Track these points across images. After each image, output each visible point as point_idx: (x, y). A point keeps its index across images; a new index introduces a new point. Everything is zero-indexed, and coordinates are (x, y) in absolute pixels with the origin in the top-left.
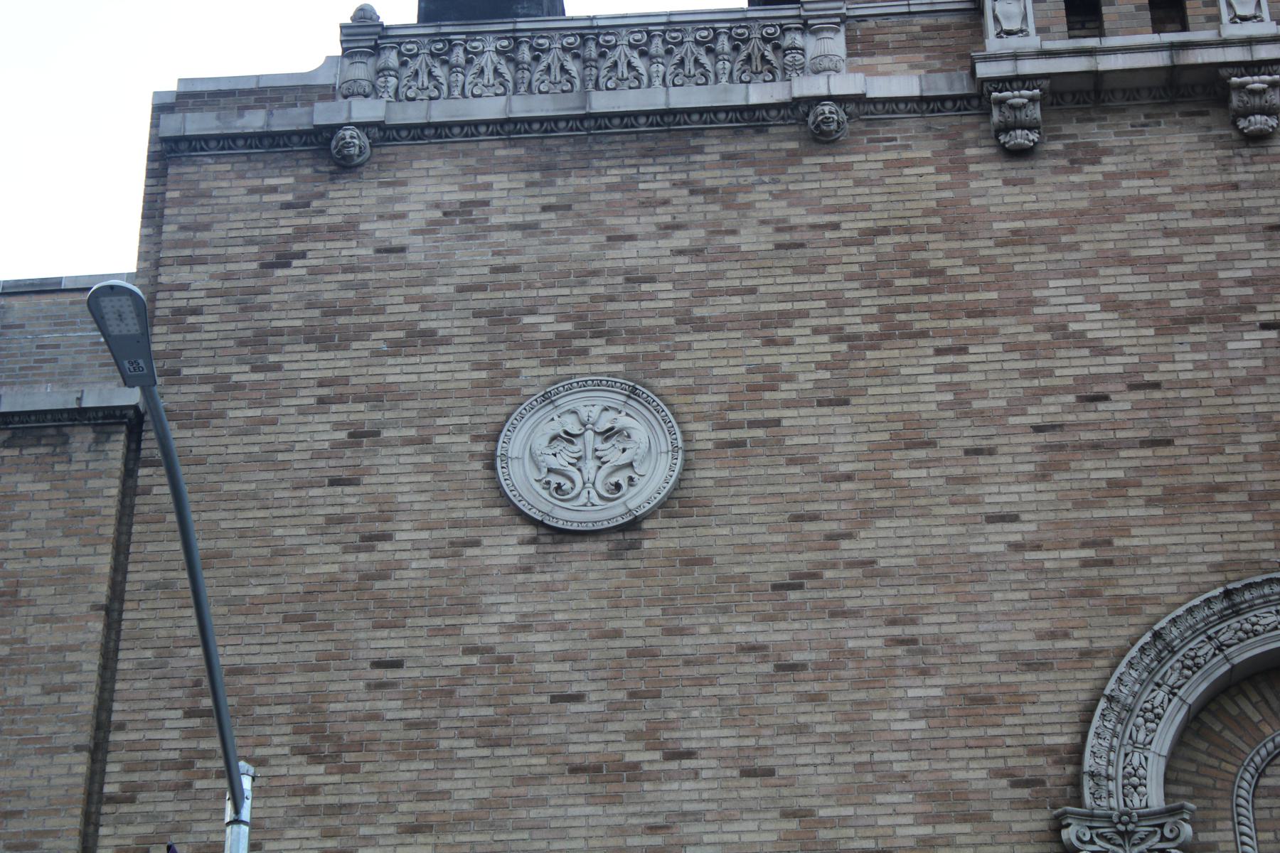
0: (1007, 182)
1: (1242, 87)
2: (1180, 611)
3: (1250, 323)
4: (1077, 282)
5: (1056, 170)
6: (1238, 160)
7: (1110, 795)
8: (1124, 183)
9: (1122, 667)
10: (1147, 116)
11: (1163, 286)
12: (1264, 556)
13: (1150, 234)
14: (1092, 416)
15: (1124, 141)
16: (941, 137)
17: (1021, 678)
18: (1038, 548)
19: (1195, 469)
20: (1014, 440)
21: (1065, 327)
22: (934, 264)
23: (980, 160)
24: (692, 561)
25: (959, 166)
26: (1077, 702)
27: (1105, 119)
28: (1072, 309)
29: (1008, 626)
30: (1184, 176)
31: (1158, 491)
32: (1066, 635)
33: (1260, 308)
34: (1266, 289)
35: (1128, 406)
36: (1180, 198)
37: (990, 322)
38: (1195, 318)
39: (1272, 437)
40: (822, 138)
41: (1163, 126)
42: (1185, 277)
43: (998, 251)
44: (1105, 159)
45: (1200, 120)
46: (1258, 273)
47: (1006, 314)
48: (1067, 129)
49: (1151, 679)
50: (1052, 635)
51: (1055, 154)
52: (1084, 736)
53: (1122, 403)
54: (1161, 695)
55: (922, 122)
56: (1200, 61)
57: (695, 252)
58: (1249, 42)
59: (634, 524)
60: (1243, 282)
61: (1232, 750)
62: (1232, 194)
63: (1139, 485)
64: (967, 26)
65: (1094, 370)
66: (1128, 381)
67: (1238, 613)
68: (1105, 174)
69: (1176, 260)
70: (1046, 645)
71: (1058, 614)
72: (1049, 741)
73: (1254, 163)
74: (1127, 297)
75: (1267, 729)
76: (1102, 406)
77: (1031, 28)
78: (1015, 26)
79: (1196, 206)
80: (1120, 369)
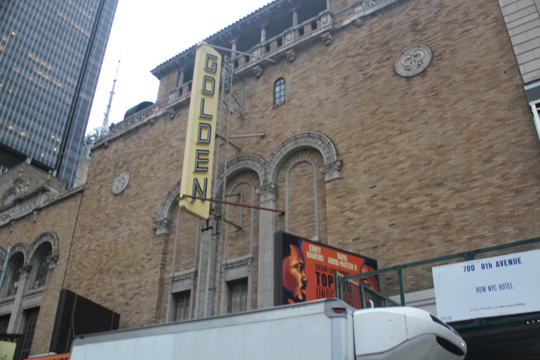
24: (128, 195)
40: (152, 124)
57: (137, 148)
59: (123, 191)
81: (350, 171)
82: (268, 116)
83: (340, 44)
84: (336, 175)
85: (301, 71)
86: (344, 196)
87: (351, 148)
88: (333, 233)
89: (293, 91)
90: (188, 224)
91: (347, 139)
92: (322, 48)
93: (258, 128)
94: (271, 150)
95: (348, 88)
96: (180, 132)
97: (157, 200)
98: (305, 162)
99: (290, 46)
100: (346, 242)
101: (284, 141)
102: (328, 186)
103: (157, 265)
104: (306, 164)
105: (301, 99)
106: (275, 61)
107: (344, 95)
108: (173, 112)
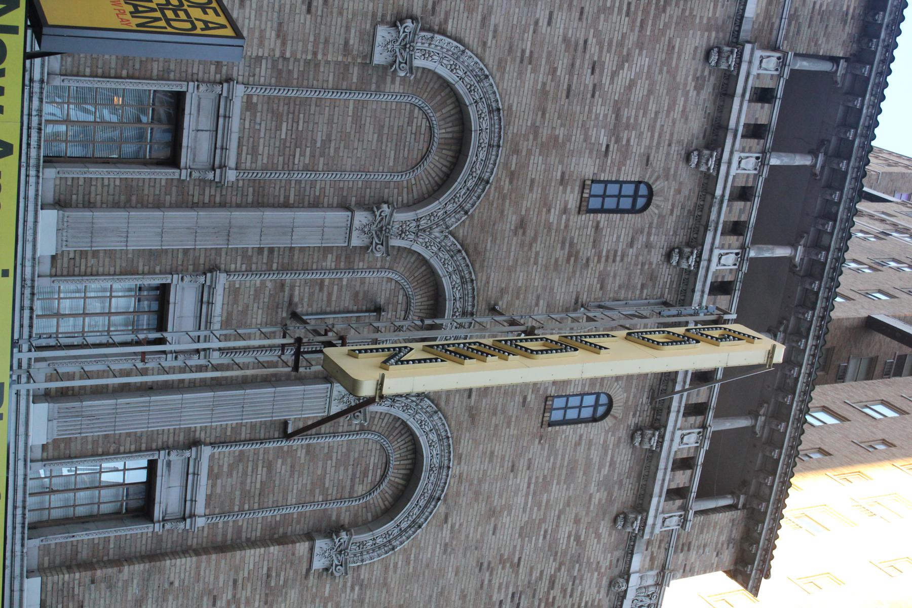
0: (696, 48)
1: (711, 156)
2: (495, 88)
4: (645, 71)
5: (696, 70)
7: (423, 43)
8: (683, 99)
9: (476, 59)
12: (511, 128)
14: (586, 66)
15: (701, 102)
16: (723, 22)
17: (480, 14)
18: (534, 32)
19: (554, 106)
20: (583, 30)
21: (627, 61)
22: (668, 9)
23: (709, 38)
25: (708, 28)
26: (465, 37)
29: (503, 12)
30: (679, 125)
31: (548, 88)
32: (494, 37)
35: (587, 82)
37: (637, 29)
38: (618, 118)
39: (560, 141)
42: (636, 117)
43: (667, 39)
44: (695, 92)
45: (701, 136)
47: (639, 36)
48: (712, 79)
49: (468, 70)
50: (495, 31)
51: (703, 71)
52: (450, 37)
53: (589, 80)
54: (461, 73)
55: (732, 16)
58: (729, 163)
60: (628, 141)
61: (432, 98)
62: (667, 142)
63: (552, 81)
64: (769, 43)
67: (489, 112)
68: (688, 92)
69: (645, 114)
70: (492, 28)
71: (504, 35)
72: (450, 21)
75: (438, 114)
76: (589, 71)
77: (761, 72)
78: (763, 65)
80: (604, 81)
81: (314, 590)
83: (601, 549)
84: (319, 564)
85: (596, 459)
86: (267, 583)
87: (361, 589)
88: (198, 567)
89: (559, 444)
90: (370, 134)
91: (385, 579)
94: (447, 402)
97: (484, 20)
98: (384, 476)
99: (666, 445)
100: (170, 598)
101: (451, 442)
102: (302, 548)
103: (284, 44)
104: (378, 479)
105: (528, 468)
107: (482, 564)
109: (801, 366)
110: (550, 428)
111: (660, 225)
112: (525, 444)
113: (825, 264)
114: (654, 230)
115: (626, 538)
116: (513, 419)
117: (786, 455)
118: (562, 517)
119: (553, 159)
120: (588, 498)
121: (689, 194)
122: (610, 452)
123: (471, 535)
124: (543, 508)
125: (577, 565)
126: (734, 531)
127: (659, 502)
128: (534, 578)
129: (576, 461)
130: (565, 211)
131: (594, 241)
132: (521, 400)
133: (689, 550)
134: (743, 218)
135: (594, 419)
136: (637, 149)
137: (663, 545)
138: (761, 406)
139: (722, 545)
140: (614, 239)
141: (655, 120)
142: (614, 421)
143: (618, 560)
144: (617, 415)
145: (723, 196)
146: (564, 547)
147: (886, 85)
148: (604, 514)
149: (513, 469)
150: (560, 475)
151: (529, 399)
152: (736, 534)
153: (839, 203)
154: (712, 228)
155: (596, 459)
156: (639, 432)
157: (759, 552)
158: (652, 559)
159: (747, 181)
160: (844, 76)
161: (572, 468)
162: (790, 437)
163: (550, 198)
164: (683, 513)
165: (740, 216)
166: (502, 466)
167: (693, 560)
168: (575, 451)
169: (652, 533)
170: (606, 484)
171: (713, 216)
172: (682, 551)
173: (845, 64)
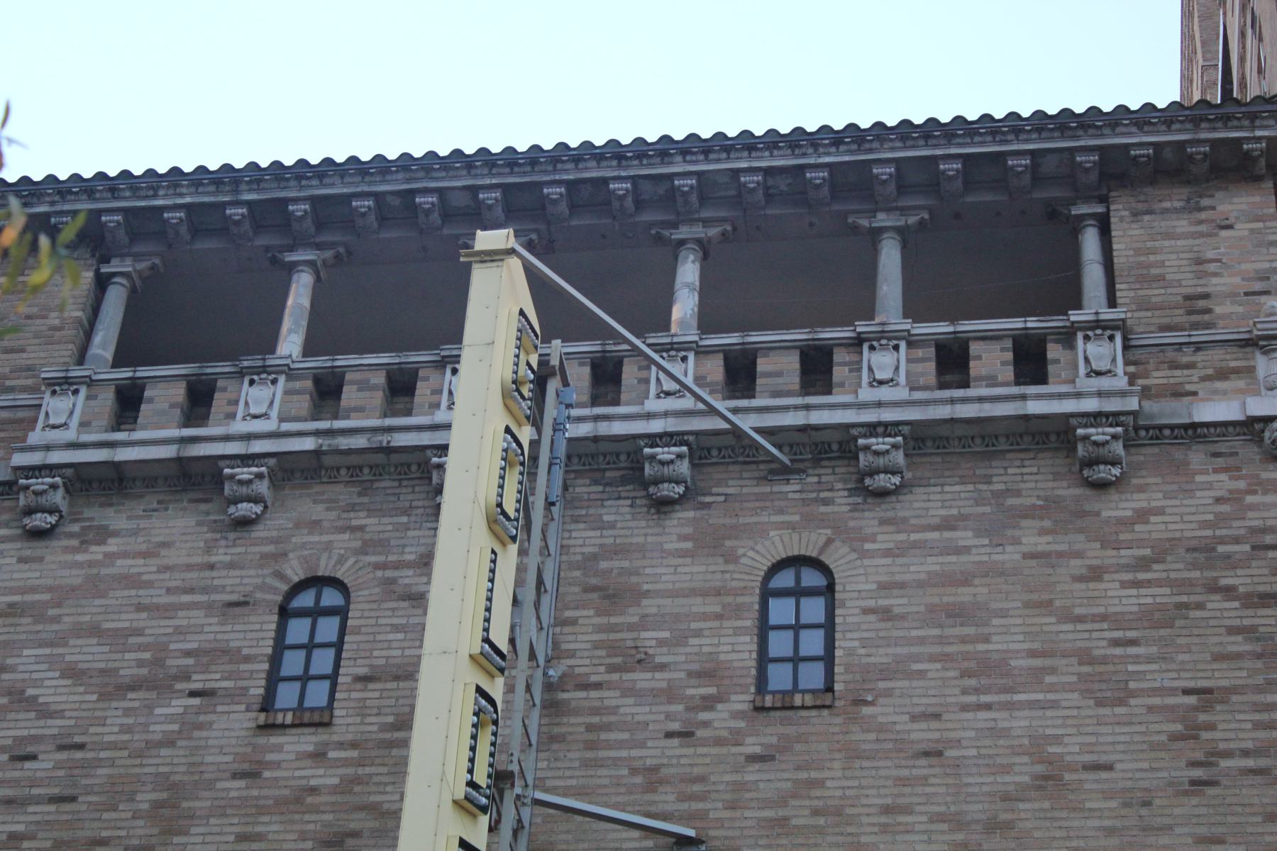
0: (22, 560)
3: (181, 691)
4: (47, 651)
5: (66, 550)
6: (223, 543)
8: (119, 562)
10: (159, 502)
11: (119, 656)
13: (124, 609)
14: (17, 774)
15: (132, 525)
21: (23, 692)
27: (123, 504)
28: (35, 676)
30: (173, 557)
33: (195, 677)
34: (205, 660)
36: (162, 576)
38: (132, 688)
39: (165, 795)
41: (170, 512)
42: (140, 648)
44: (110, 541)
45: (203, 507)
46: (203, 645)
48: (87, 513)
51: (71, 535)
53: (45, 764)
56: (202, 453)
60: (188, 654)
62: (207, 574)
63: (33, 837)
65: (33, 732)
66: (58, 742)
69: (139, 632)
73: (234, 546)
74: (85, 666)
76: (28, 765)
79: (173, 584)
80: (55, 731)
82: (719, 742)
83: (1175, 504)
85: (933, 564)
89: (881, 656)
92: (1068, 491)
93: (651, 787)
95: (1214, 755)
96: (94, 631)
99: (889, 415)
105: (937, 716)
106: (785, 459)
107: (1194, 782)
108: (58, 498)
109: (736, 172)
110: (837, 687)
111: (381, 544)
112: (872, 736)
113: (505, 188)
114: (391, 558)
115: (1156, 450)
116: (803, 775)
117: (950, 143)
118: (1078, 611)
119: (200, 805)
120: (1033, 563)
121: (322, 502)
122: (914, 537)
123: (1108, 823)
124: (1048, 662)
125: (1221, 549)
126: (1167, 204)
127: (1039, 397)
128: (1248, 648)
129: (931, 609)
130: (318, 756)
131: (397, 678)
132: (757, 766)
133: (1206, 296)
134: (380, 379)
135: (829, 590)
136: (213, 630)
137: (1185, 359)
138: (855, 229)
139: (1200, 222)
140: (400, 636)
141: (157, 607)
142: (838, 543)
143: (1216, 455)
144: (822, 540)
145: (317, 433)
146: (1167, 591)
147: (150, 173)
148: (1082, 514)
149: (933, 754)
150: (963, 640)
151: (758, 750)
152: (1176, 198)
153: (377, 196)
154: (384, 439)
155: (933, 564)
156: (868, 481)
157: (1203, 136)
158: (1223, 374)
159: (298, 392)
160: (137, 257)
161: (949, 616)
162: (905, 148)
163: (286, 792)
164: (1080, 335)
165: (374, 388)
166: (924, 780)
167: (1237, 280)
168: (903, 617)
169: (1123, 394)
170: (997, 529)
171: (360, 442)
172: (1208, 311)
173: (115, 261)
